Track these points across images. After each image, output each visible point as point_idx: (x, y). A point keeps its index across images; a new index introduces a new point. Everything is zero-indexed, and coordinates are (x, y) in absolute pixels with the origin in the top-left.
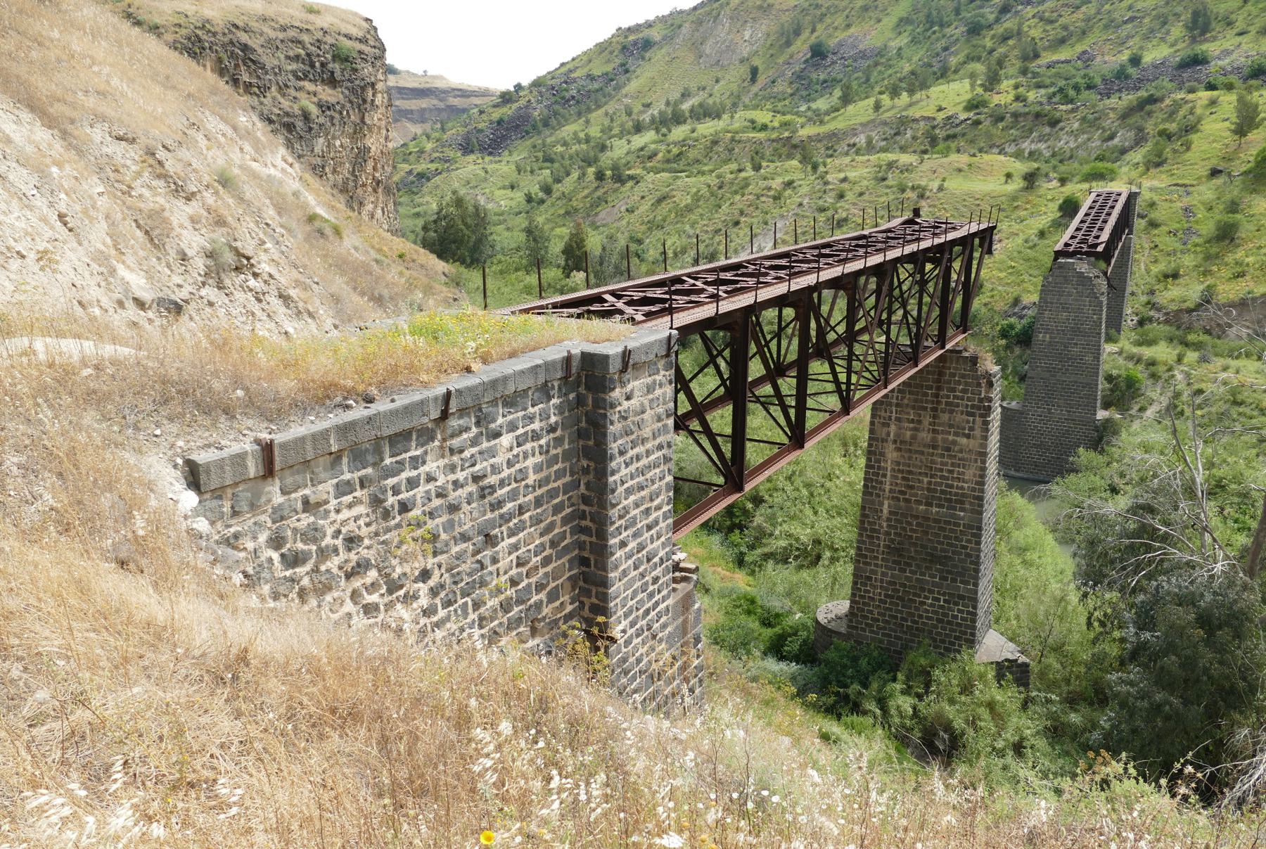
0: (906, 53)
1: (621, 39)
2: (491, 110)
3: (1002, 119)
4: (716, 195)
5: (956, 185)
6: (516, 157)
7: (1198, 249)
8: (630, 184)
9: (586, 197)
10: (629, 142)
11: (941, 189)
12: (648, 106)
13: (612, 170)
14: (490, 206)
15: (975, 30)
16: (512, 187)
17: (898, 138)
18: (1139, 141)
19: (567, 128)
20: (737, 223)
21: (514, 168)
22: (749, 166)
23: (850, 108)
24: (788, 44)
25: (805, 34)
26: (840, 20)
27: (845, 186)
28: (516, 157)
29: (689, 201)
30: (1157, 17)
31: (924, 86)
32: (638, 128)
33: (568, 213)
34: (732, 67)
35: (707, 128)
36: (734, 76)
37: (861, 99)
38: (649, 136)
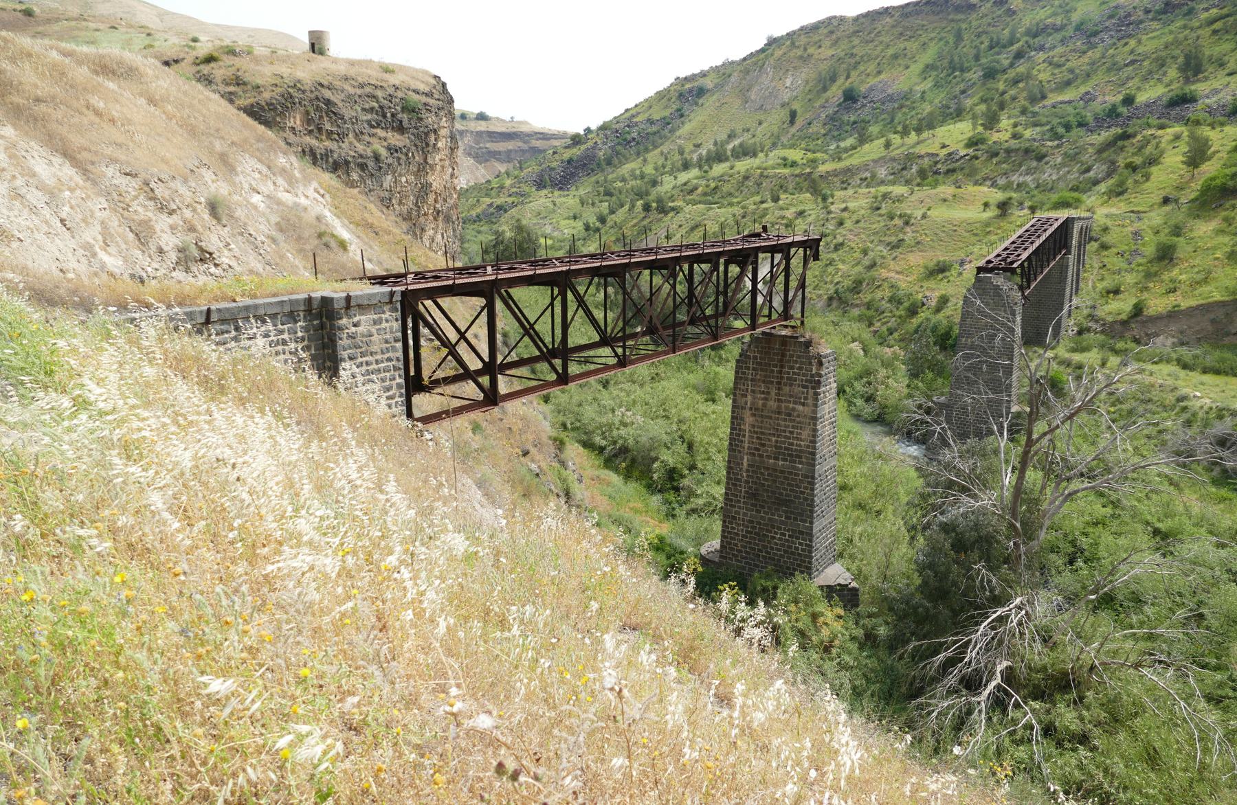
3: (997, 154)
6: (582, 192)
7: (1141, 268)
8: (672, 214)
10: (676, 178)
16: (575, 218)
28: (582, 192)
30: (1157, 60)
32: (686, 166)
35: (742, 165)
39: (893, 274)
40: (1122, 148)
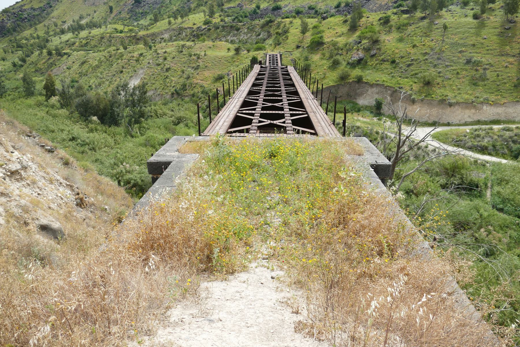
3: (218, 28)
5: (209, 53)
8: (66, 57)
9: (44, 63)
10: (60, 38)
11: (205, 55)
12: (64, 22)
16: (4, 60)
17: (180, 36)
18: (269, 36)
19: (26, 32)
20: (122, 72)
22: (121, 48)
23: (158, 23)
27: (166, 55)
29: (97, 63)
31: (187, 15)
32: (63, 32)
33: (36, 71)
35: (95, 32)
37: (161, 20)
38: (69, 36)
39: (199, 81)
40: (271, 26)
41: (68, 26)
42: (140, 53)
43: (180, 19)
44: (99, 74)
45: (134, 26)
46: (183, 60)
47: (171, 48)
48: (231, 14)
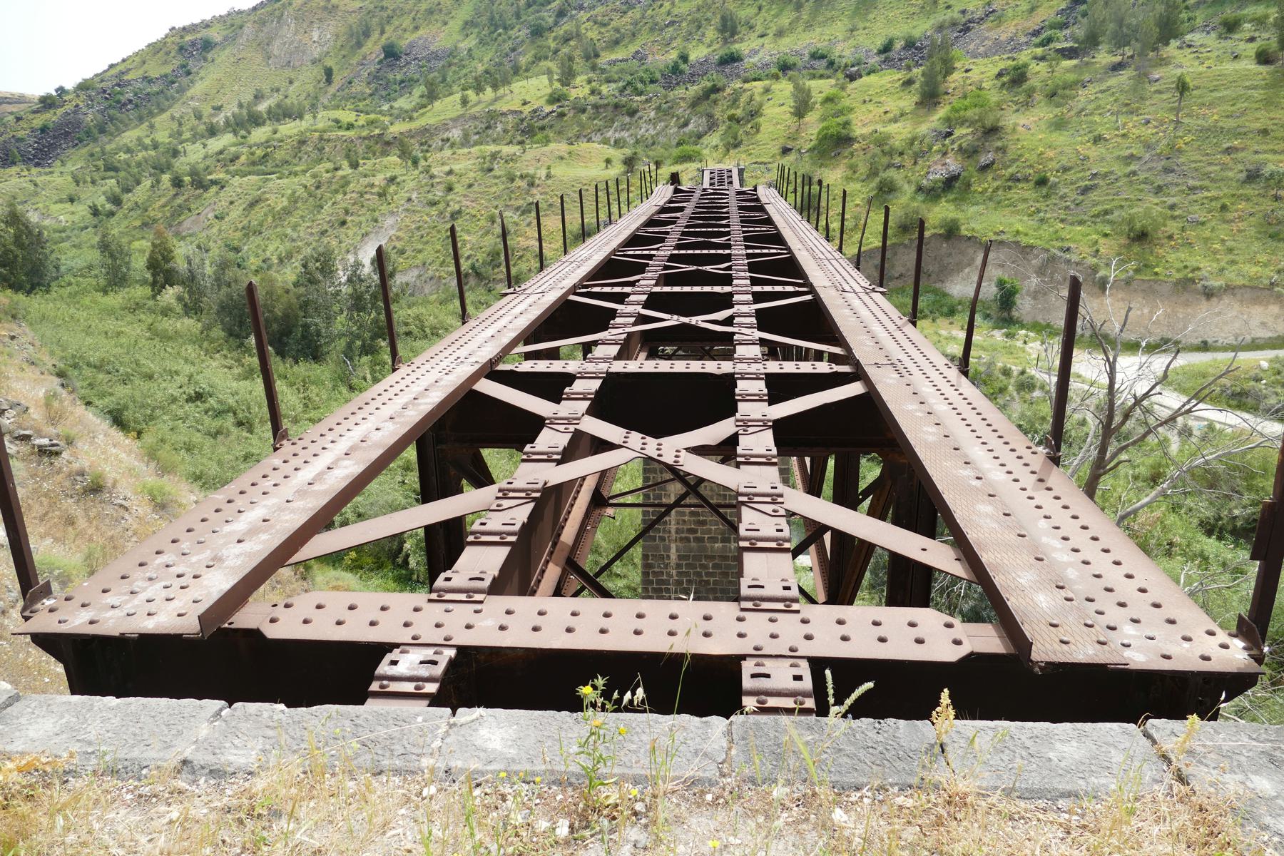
0: (476, 53)
1: (177, 39)
2: (31, 116)
3: (584, 111)
4: (316, 196)
5: (559, 171)
8: (214, 189)
9: (164, 206)
10: (205, 146)
11: (548, 176)
12: (219, 108)
13: (191, 175)
14: (47, 222)
15: (538, 32)
16: (72, 200)
17: (490, 132)
18: (712, 125)
20: (343, 223)
21: (70, 179)
22: (345, 164)
23: (437, 104)
24: (359, 45)
25: (375, 35)
26: (407, 22)
27: (452, 178)
28: (70, 167)
29: (286, 203)
31: (506, 82)
32: (212, 132)
33: (145, 225)
34: (304, 68)
35: (289, 129)
36: (308, 78)
38: (226, 139)
41: (227, 118)
42: (388, 175)
43: (489, 93)
44: (289, 231)
45: (381, 112)
46: (494, 189)
47: (465, 162)
48: (616, 77)
